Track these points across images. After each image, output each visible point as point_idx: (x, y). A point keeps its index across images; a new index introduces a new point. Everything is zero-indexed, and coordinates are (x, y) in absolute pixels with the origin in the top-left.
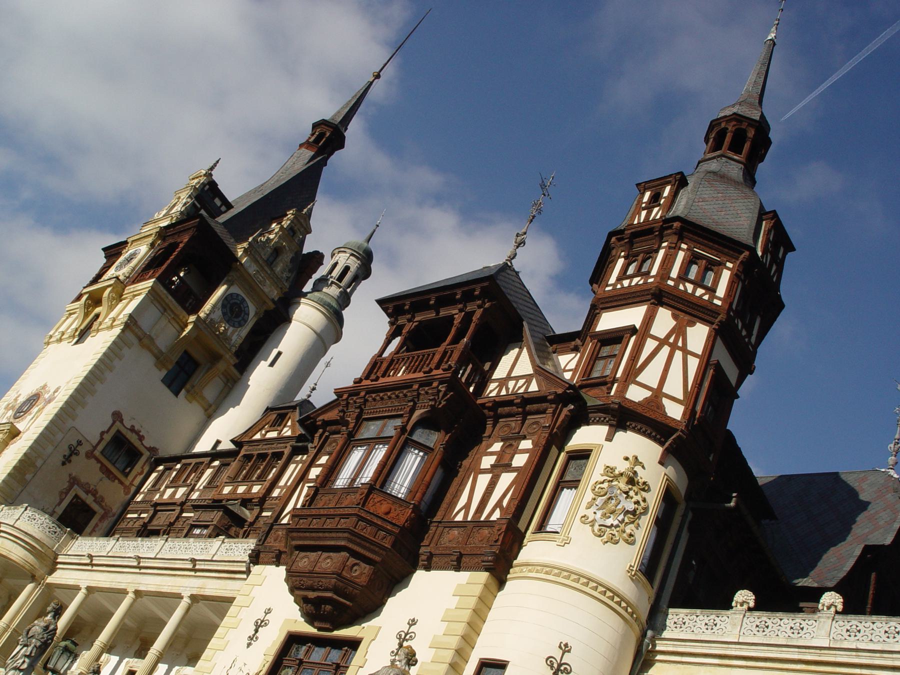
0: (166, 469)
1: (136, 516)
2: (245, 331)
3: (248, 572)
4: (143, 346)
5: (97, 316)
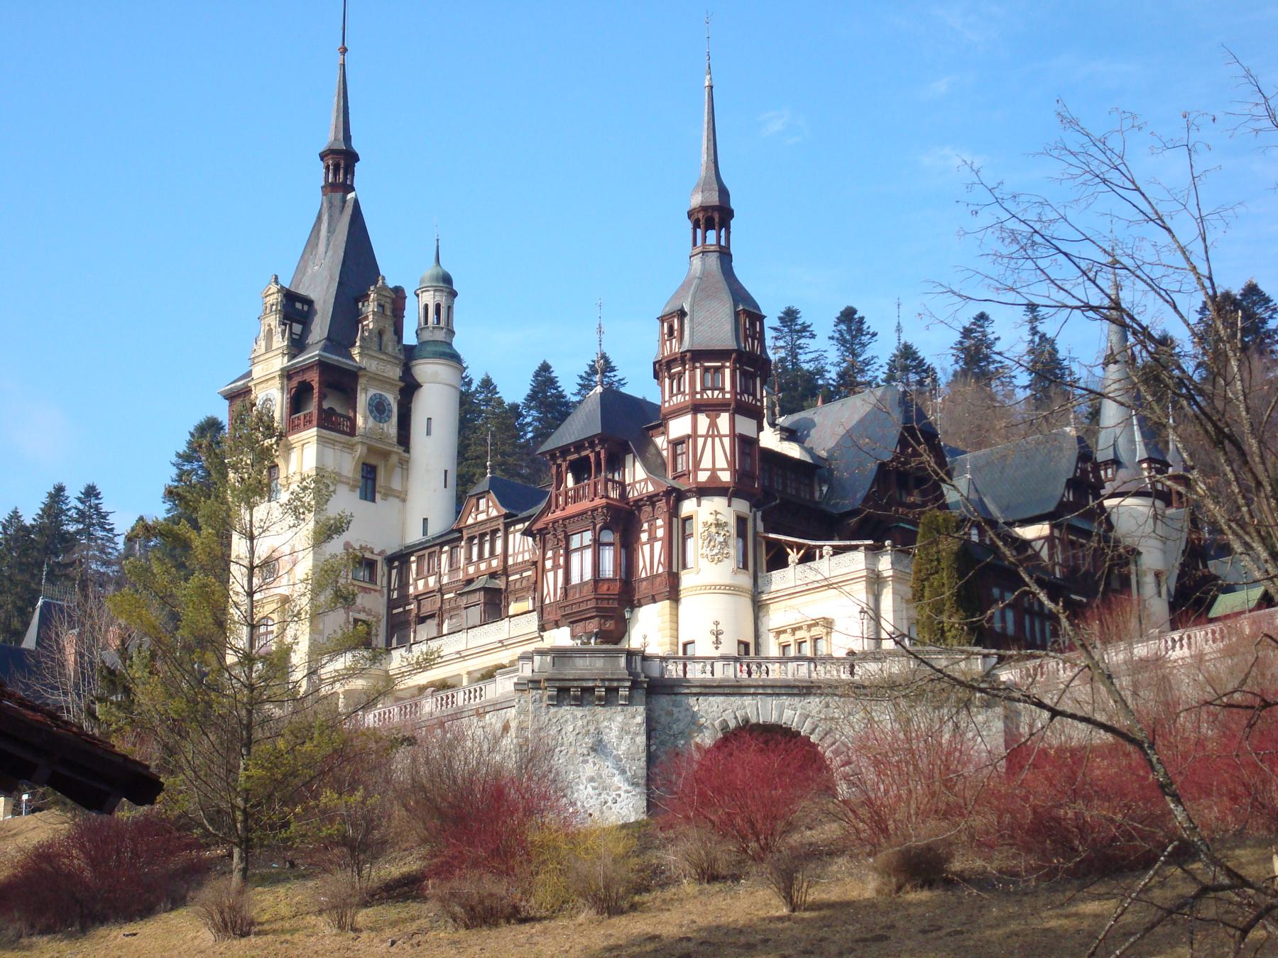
0: (402, 564)
1: (401, 610)
2: (394, 419)
3: (542, 637)
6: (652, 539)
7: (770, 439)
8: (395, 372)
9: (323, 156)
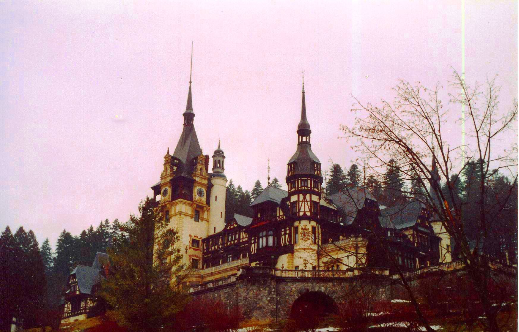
2: (205, 196)
4: (186, 216)
5: (167, 212)
6: (285, 234)
7: (323, 203)
8: (205, 182)
9: (185, 115)
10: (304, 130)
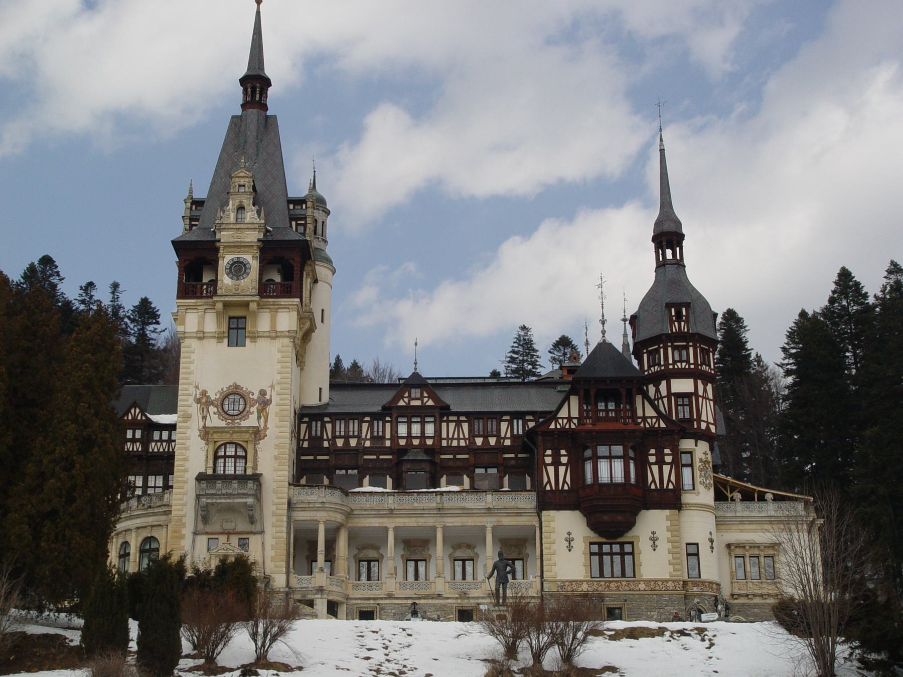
6: (660, 462)
10: (668, 237)
